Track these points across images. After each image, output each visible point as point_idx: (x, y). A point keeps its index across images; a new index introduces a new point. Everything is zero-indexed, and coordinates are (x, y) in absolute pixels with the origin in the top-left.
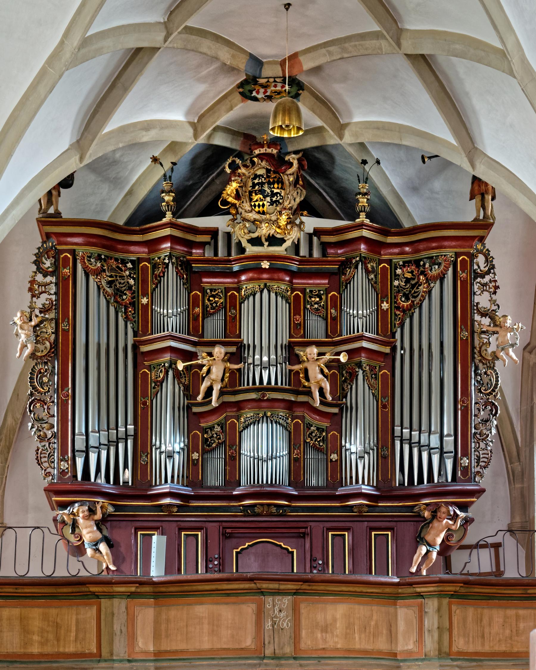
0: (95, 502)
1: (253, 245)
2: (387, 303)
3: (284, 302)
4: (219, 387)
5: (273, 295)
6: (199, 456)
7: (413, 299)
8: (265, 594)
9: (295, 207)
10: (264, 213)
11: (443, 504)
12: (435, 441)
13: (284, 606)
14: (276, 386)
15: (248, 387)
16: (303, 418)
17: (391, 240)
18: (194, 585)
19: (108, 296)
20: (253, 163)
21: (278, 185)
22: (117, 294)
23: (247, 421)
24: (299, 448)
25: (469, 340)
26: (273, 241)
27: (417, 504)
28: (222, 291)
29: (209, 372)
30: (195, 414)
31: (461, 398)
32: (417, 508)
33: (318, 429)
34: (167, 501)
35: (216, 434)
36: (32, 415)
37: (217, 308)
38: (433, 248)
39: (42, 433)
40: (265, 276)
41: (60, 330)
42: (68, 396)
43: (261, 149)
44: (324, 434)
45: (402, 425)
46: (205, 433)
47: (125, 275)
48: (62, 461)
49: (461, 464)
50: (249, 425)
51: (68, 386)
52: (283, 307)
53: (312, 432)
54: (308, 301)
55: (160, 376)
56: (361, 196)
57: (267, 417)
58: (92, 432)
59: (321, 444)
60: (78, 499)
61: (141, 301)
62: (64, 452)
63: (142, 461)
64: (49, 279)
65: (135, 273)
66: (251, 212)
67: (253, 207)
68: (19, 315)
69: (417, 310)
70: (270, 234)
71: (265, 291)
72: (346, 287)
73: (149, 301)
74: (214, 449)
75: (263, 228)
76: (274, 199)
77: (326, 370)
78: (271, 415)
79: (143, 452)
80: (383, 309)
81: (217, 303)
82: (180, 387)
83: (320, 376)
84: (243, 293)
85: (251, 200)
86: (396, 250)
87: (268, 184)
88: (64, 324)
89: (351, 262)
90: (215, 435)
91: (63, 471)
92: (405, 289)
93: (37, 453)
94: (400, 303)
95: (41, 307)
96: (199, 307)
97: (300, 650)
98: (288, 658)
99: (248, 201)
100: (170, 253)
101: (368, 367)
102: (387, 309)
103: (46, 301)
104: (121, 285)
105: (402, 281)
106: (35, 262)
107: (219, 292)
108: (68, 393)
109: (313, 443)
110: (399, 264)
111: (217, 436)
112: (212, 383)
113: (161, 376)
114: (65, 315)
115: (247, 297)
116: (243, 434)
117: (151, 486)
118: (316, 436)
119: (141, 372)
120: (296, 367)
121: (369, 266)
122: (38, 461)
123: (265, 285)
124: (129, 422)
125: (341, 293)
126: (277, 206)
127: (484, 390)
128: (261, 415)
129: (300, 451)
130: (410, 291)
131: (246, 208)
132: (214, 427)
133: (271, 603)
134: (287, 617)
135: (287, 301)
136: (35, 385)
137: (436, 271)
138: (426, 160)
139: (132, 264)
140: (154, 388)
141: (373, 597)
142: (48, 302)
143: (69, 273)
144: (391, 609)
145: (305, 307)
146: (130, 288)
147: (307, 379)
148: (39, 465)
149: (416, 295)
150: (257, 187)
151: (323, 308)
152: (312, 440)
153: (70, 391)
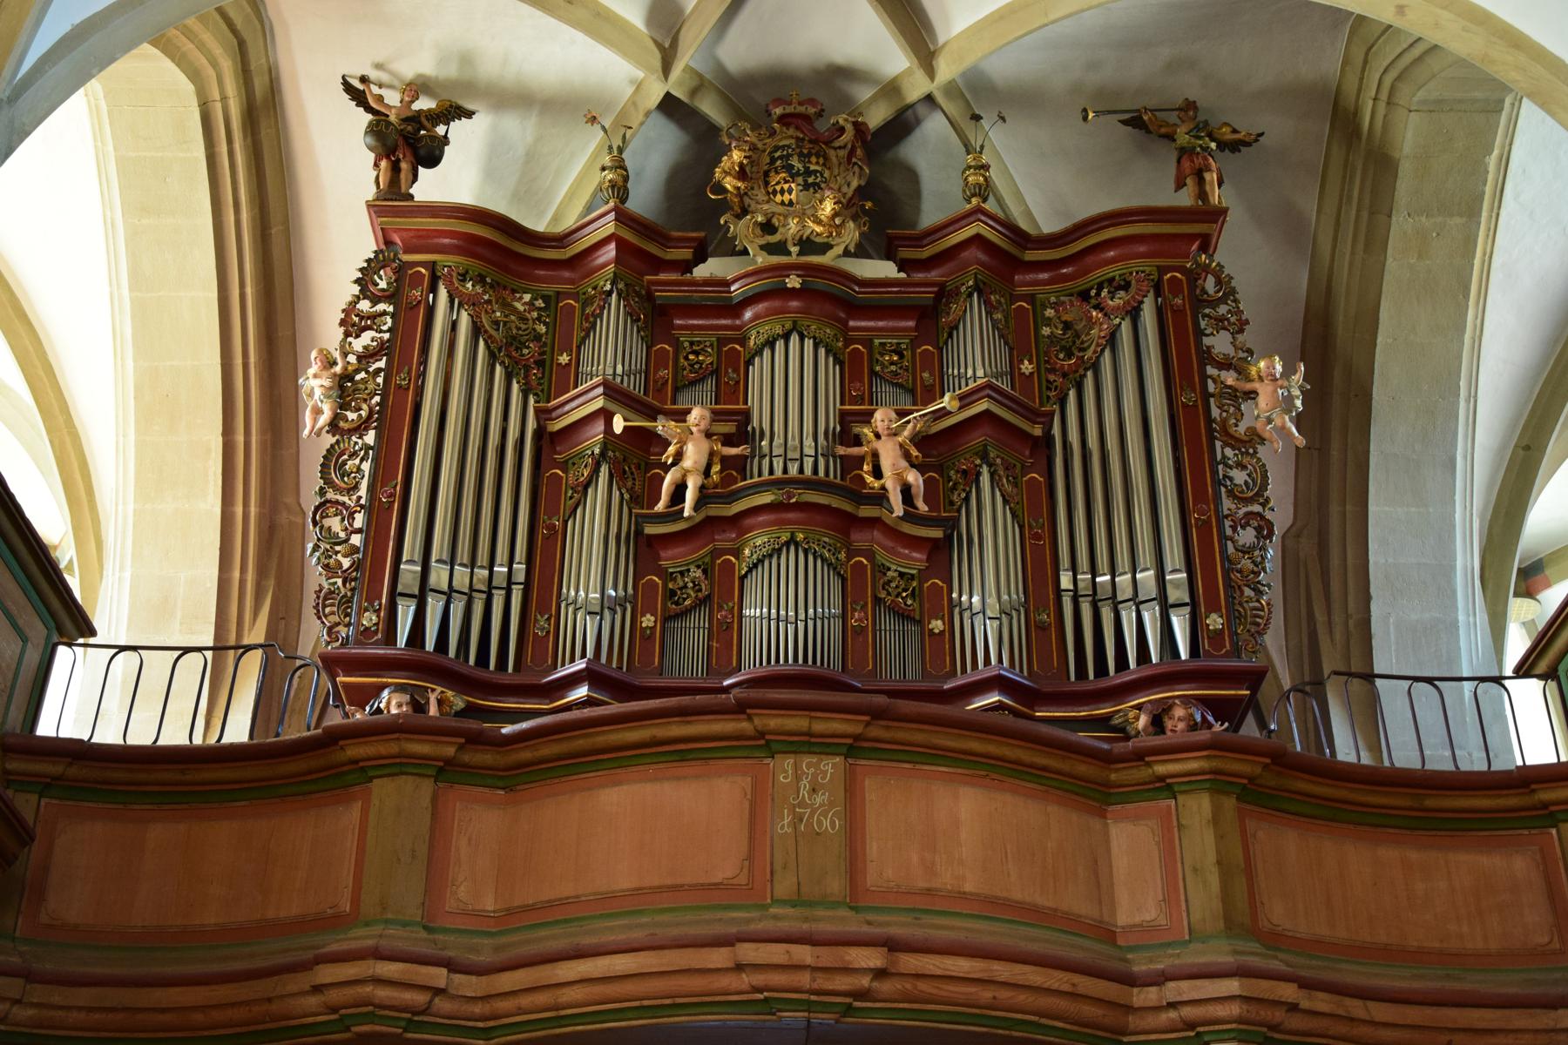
0: (426, 688)
1: (771, 253)
2: (1031, 362)
3: (831, 359)
4: (699, 483)
5: (809, 344)
6: (655, 622)
7: (1081, 354)
8: (775, 746)
9: (850, 194)
10: (791, 203)
11: (1177, 701)
12: (1147, 577)
13: (823, 778)
14: (814, 477)
15: (760, 479)
16: (870, 555)
17: (1031, 256)
18: (598, 734)
19: (492, 343)
20: (773, 133)
21: (818, 158)
22: (512, 344)
23: (756, 552)
24: (864, 607)
25: (1200, 407)
26: (808, 245)
27: (1119, 711)
28: (712, 345)
29: (679, 456)
30: (651, 537)
31: (1194, 505)
32: (1120, 717)
33: (902, 575)
34: (582, 692)
35: (693, 582)
36: (317, 529)
37: (702, 371)
38: (1113, 261)
39: (332, 561)
40: (794, 304)
41: (393, 386)
42: (392, 495)
43: (786, 107)
44: (915, 584)
45: (1074, 568)
46: (671, 580)
47: (530, 318)
48: (366, 610)
49: (1208, 625)
50: (760, 561)
51: (397, 478)
52: (830, 374)
53: (890, 581)
54: (877, 360)
55: (583, 475)
56: (972, 170)
57: (797, 545)
58: (437, 561)
59: (909, 602)
60: (390, 680)
61: (558, 359)
62: (373, 595)
63: (538, 629)
64: (381, 307)
65: (548, 316)
66: (768, 202)
67: (771, 196)
68: (314, 354)
69: (1089, 374)
70: (802, 236)
71: (795, 339)
72: (950, 335)
73: (571, 359)
74: (687, 612)
75: (788, 227)
76: (810, 180)
77: (915, 452)
78: (805, 539)
79: (540, 613)
80: (1024, 373)
81: (702, 364)
82: (622, 495)
83: (904, 464)
84: (752, 343)
85: (767, 184)
86: (1044, 276)
87: (799, 156)
88: (400, 377)
89: (958, 293)
90: (691, 585)
91: (367, 629)
92: (1063, 339)
93: (318, 597)
94: (1057, 363)
95: (361, 350)
96: (667, 368)
97: (868, 890)
98: (835, 905)
99: (762, 187)
100: (615, 273)
101: (998, 461)
102: (1032, 374)
103: (372, 341)
104: (520, 332)
105: (1057, 328)
106: (357, 281)
107: (706, 346)
108: (395, 490)
109: (892, 601)
110: (1049, 301)
111: (695, 585)
112: (684, 476)
113: (585, 475)
114: (405, 360)
115: (759, 352)
116: (747, 582)
117: (556, 668)
118: (897, 587)
119: (547, 475)
120: (855, 451)
121: (992, 297)
122: (318, 611)
123: (795, 323)
124: (517, 558)
125: (941, 345)
126: (815, 192)
127: (1240, 492)
128: (784, 538)
129: (866, 614)
130: (1074, 342)
131: (757, 198)
132: (689, 570)
133: (790, 772)
134: (831, 804)
135: (837, 361)
136: (332, 478)
137: (1120, 299)
138: (1091, 115)
139: (544, 302)
140: (571, 498)
141: (1044, 781)
142: (375, 343)
143: (421, 296)
144: (1096, 823)
145: (873, 373)
146: (538, 337)
147: (877, 473)
148: (319, 618)
149: (1086, 345)
150: (778, 163)
151: (907, 370)
152: (889, 594)
153: (398, 488)
